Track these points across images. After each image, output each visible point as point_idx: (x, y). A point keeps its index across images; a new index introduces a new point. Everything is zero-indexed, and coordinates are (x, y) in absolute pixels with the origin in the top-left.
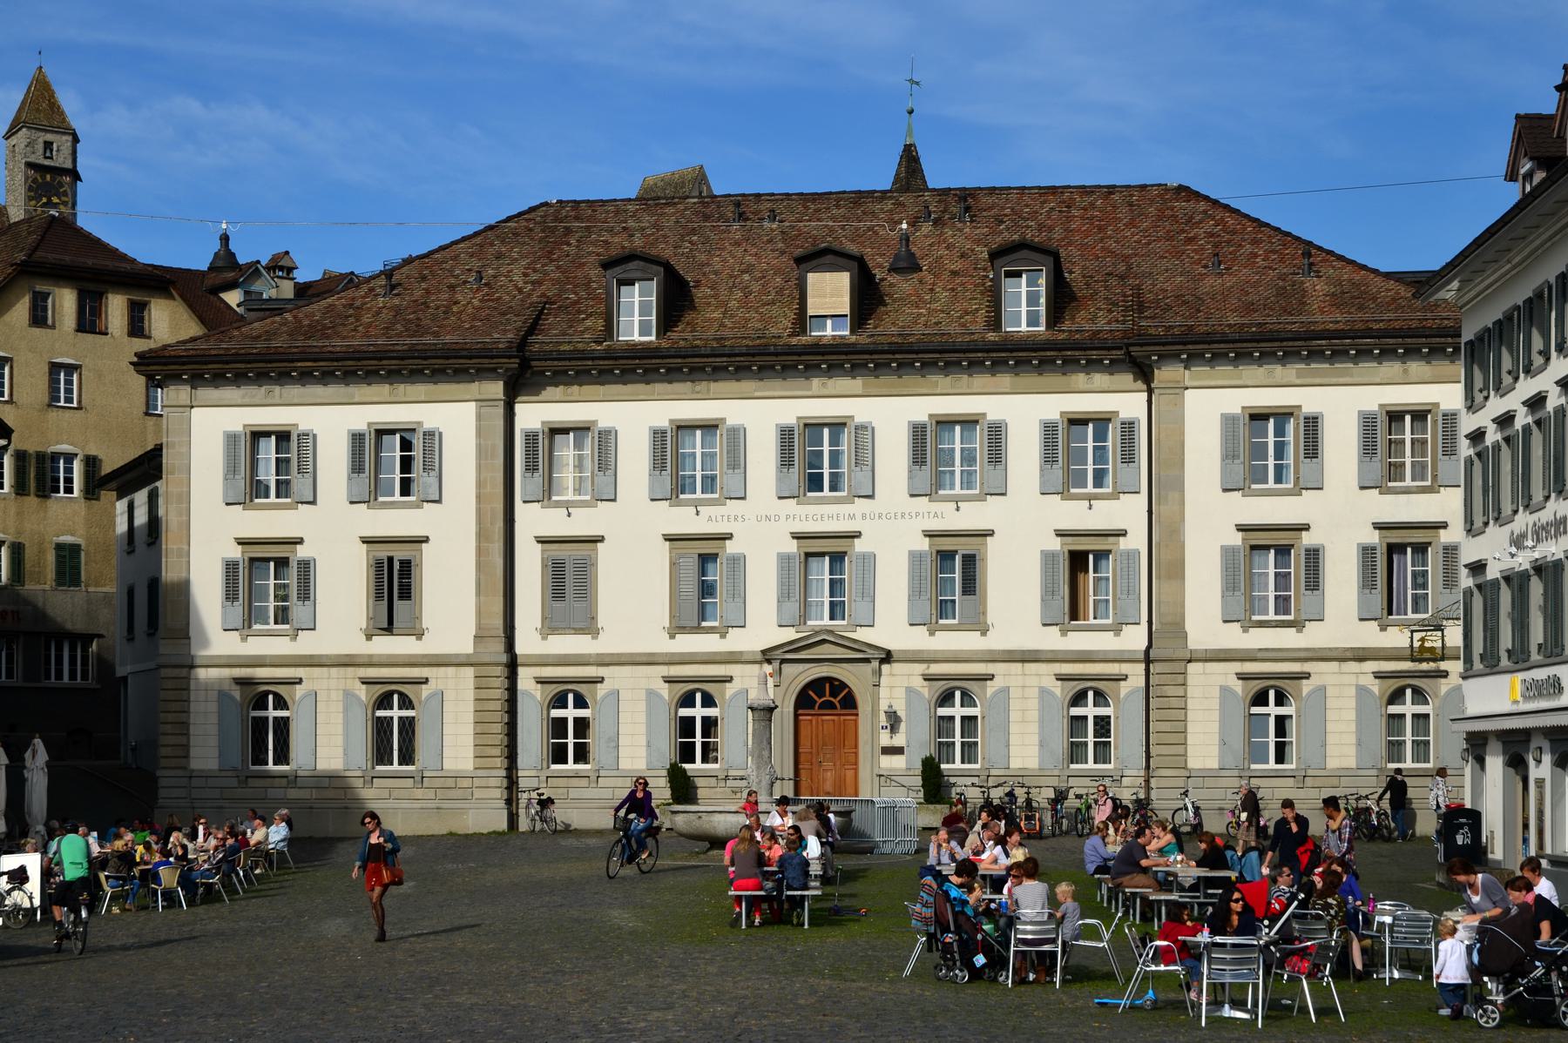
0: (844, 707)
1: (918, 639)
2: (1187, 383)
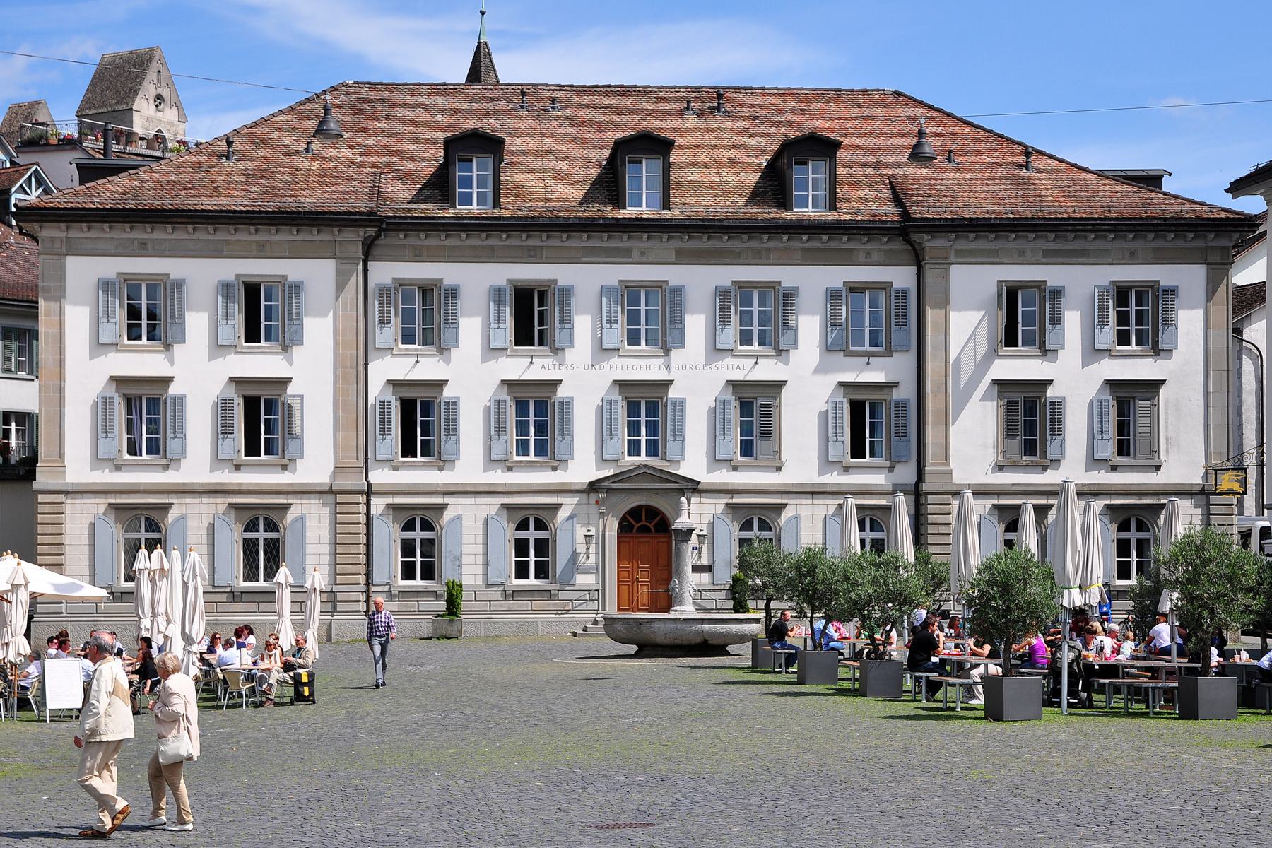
0: (657, 531)
2: (953, 259)
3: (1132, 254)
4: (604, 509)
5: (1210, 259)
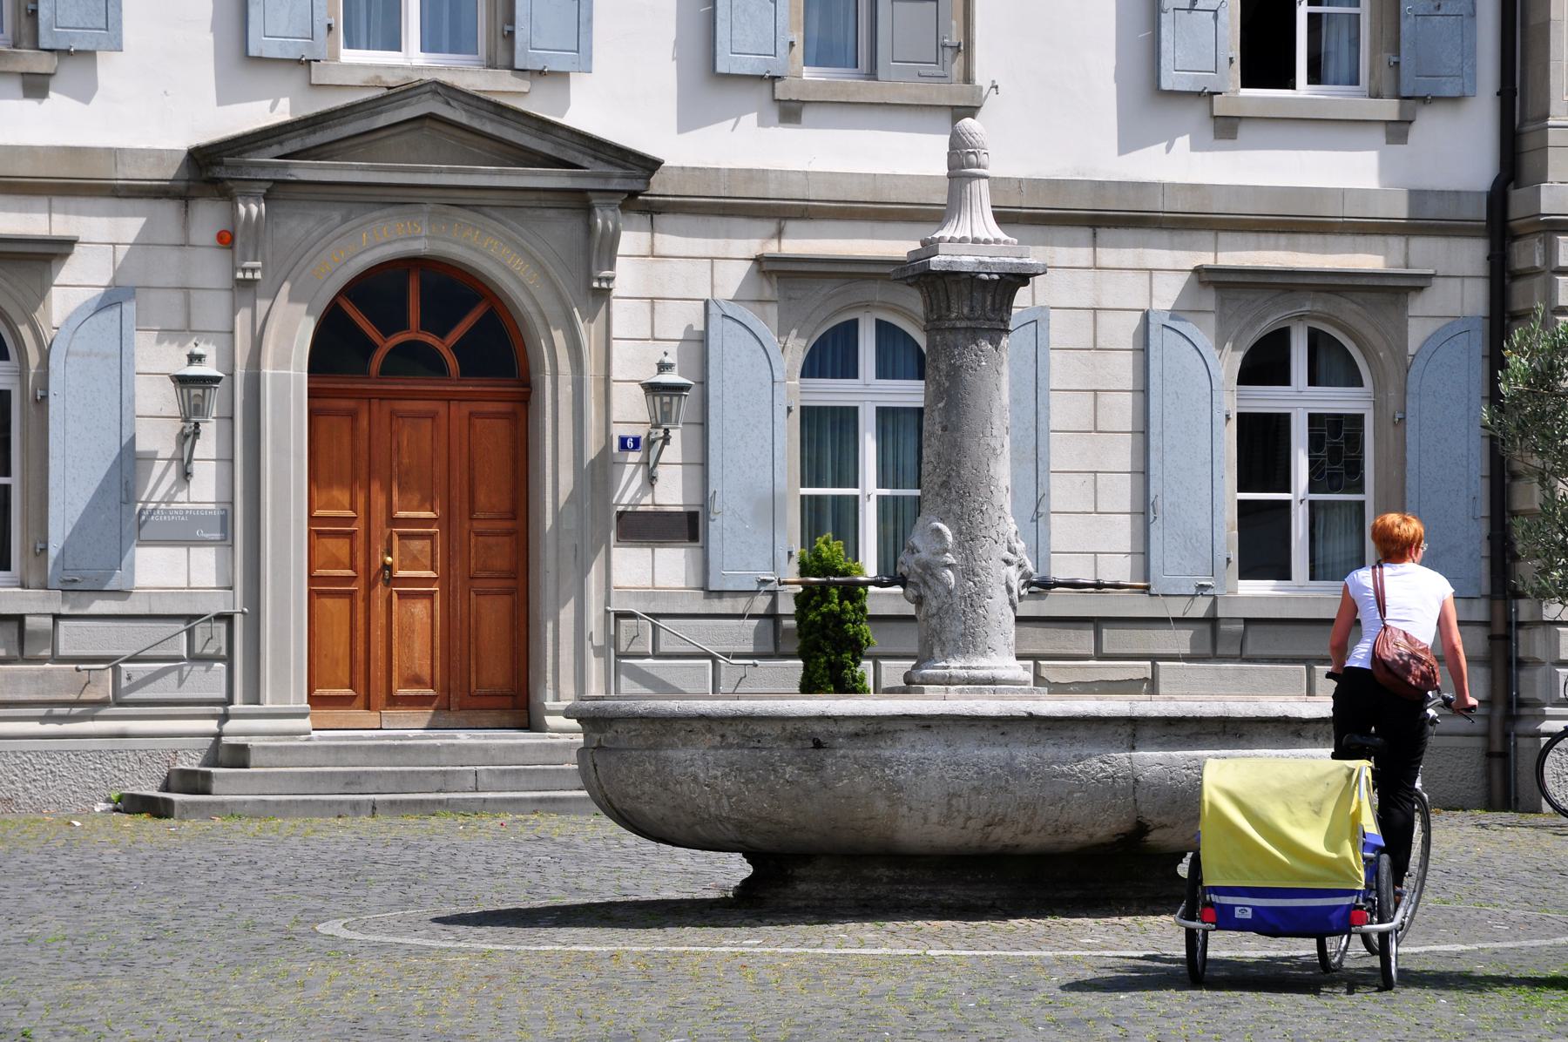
0: (467, 371)
4: (253, 267)
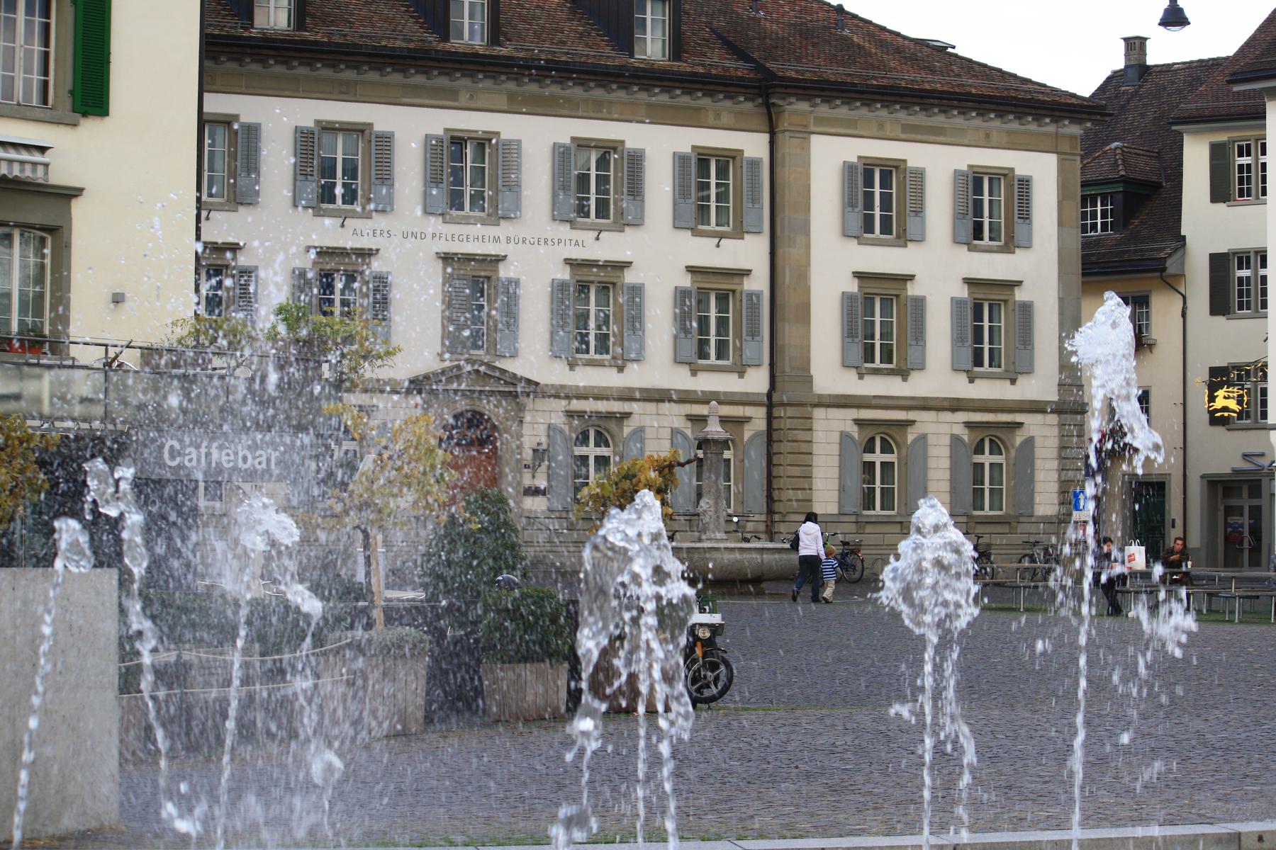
1: (554, 373)
2: (812, 128)
3: (988, 136)
5: (1060, 149)
